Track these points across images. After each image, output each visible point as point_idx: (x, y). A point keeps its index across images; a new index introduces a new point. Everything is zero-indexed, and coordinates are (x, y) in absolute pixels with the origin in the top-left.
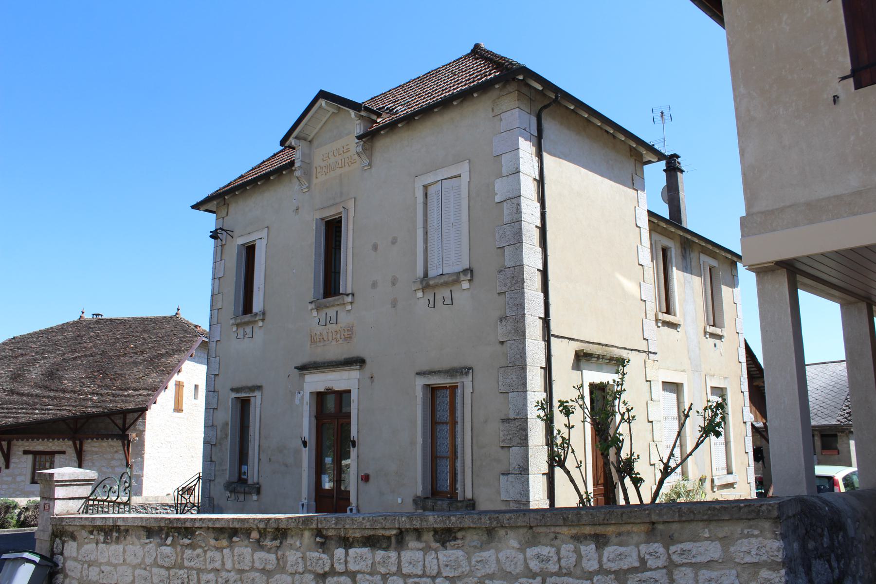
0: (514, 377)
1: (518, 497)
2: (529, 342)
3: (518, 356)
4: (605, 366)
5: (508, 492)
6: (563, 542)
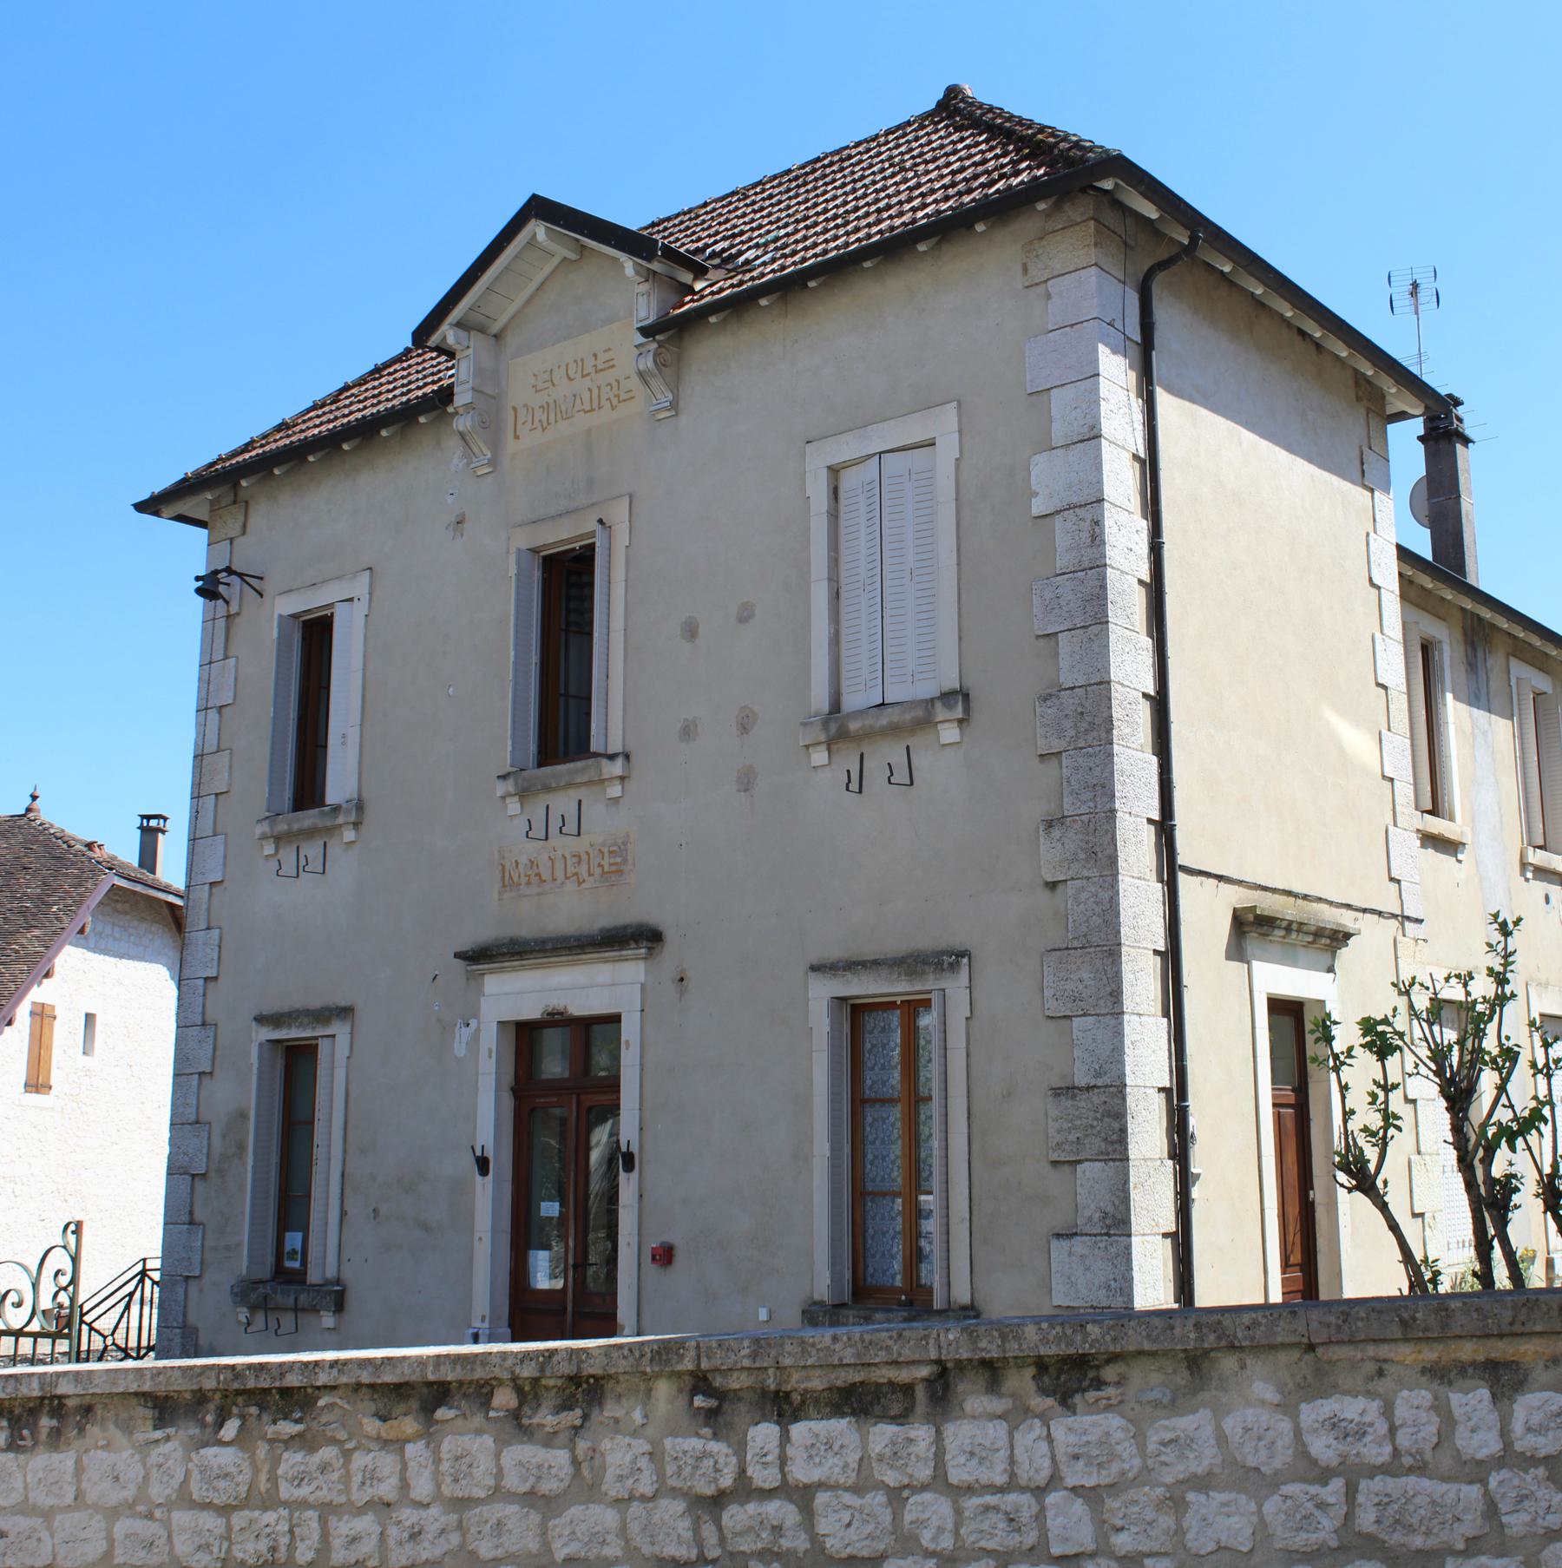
0: (1086, 975)
1: (1102, 1298)
2: (1125, 883)
3: (1097, 921)
4: (1301, 951)
5: (1072, 1284)
6: (1401, 1383)
